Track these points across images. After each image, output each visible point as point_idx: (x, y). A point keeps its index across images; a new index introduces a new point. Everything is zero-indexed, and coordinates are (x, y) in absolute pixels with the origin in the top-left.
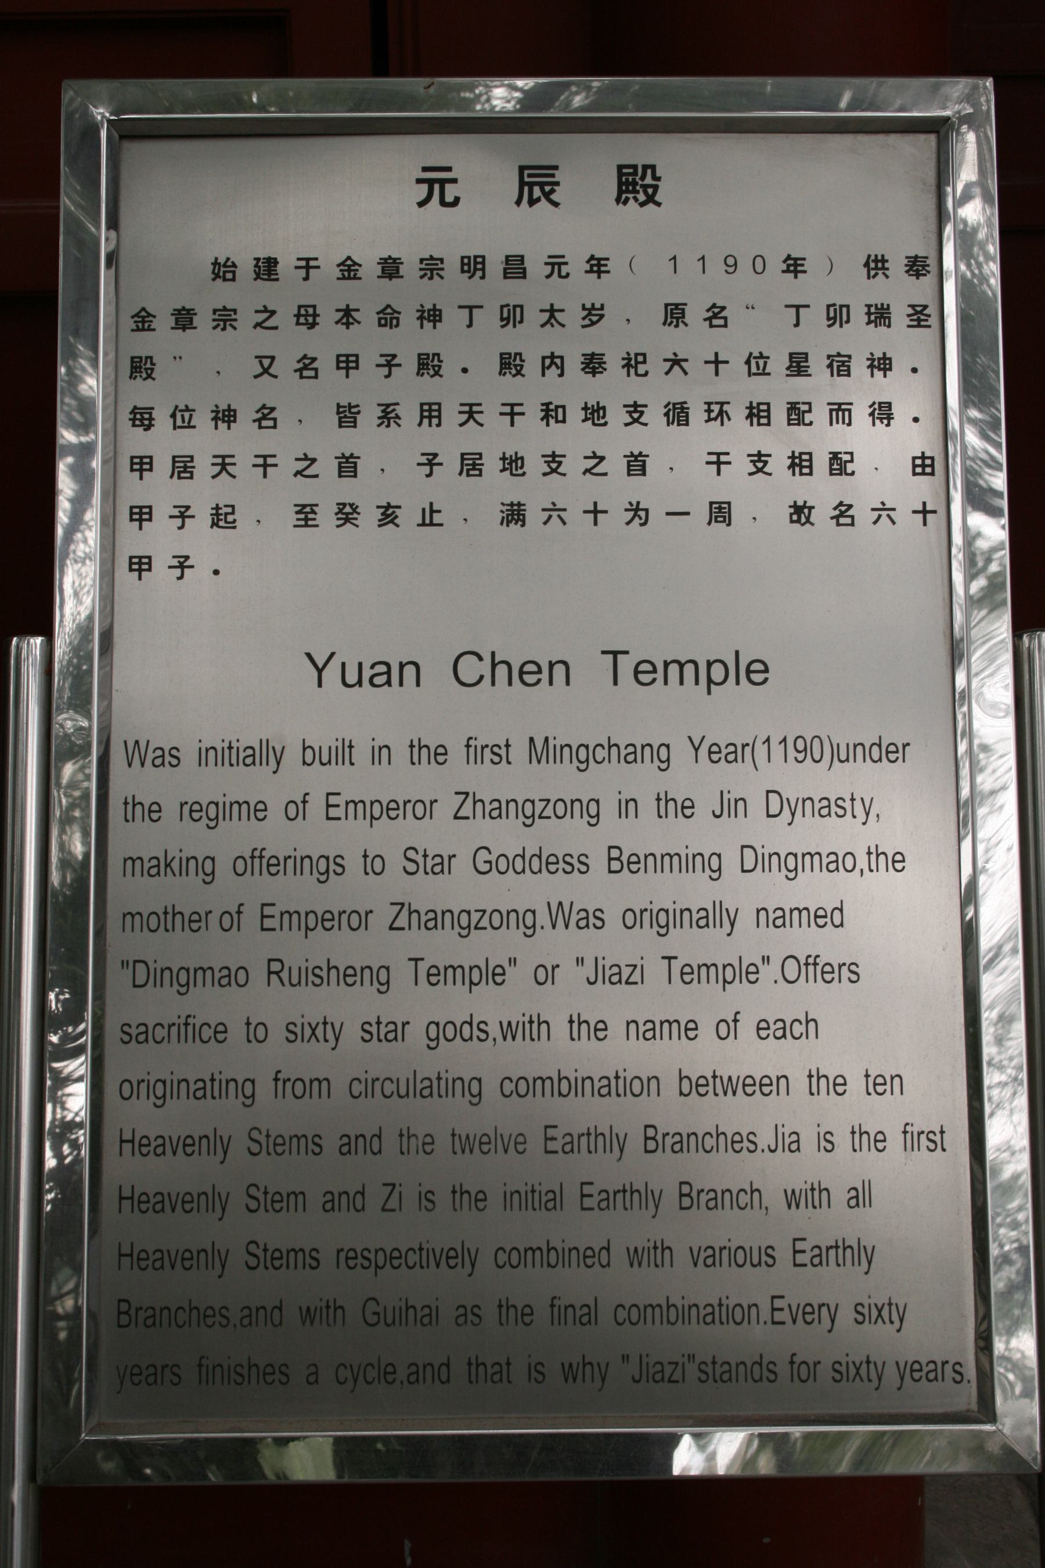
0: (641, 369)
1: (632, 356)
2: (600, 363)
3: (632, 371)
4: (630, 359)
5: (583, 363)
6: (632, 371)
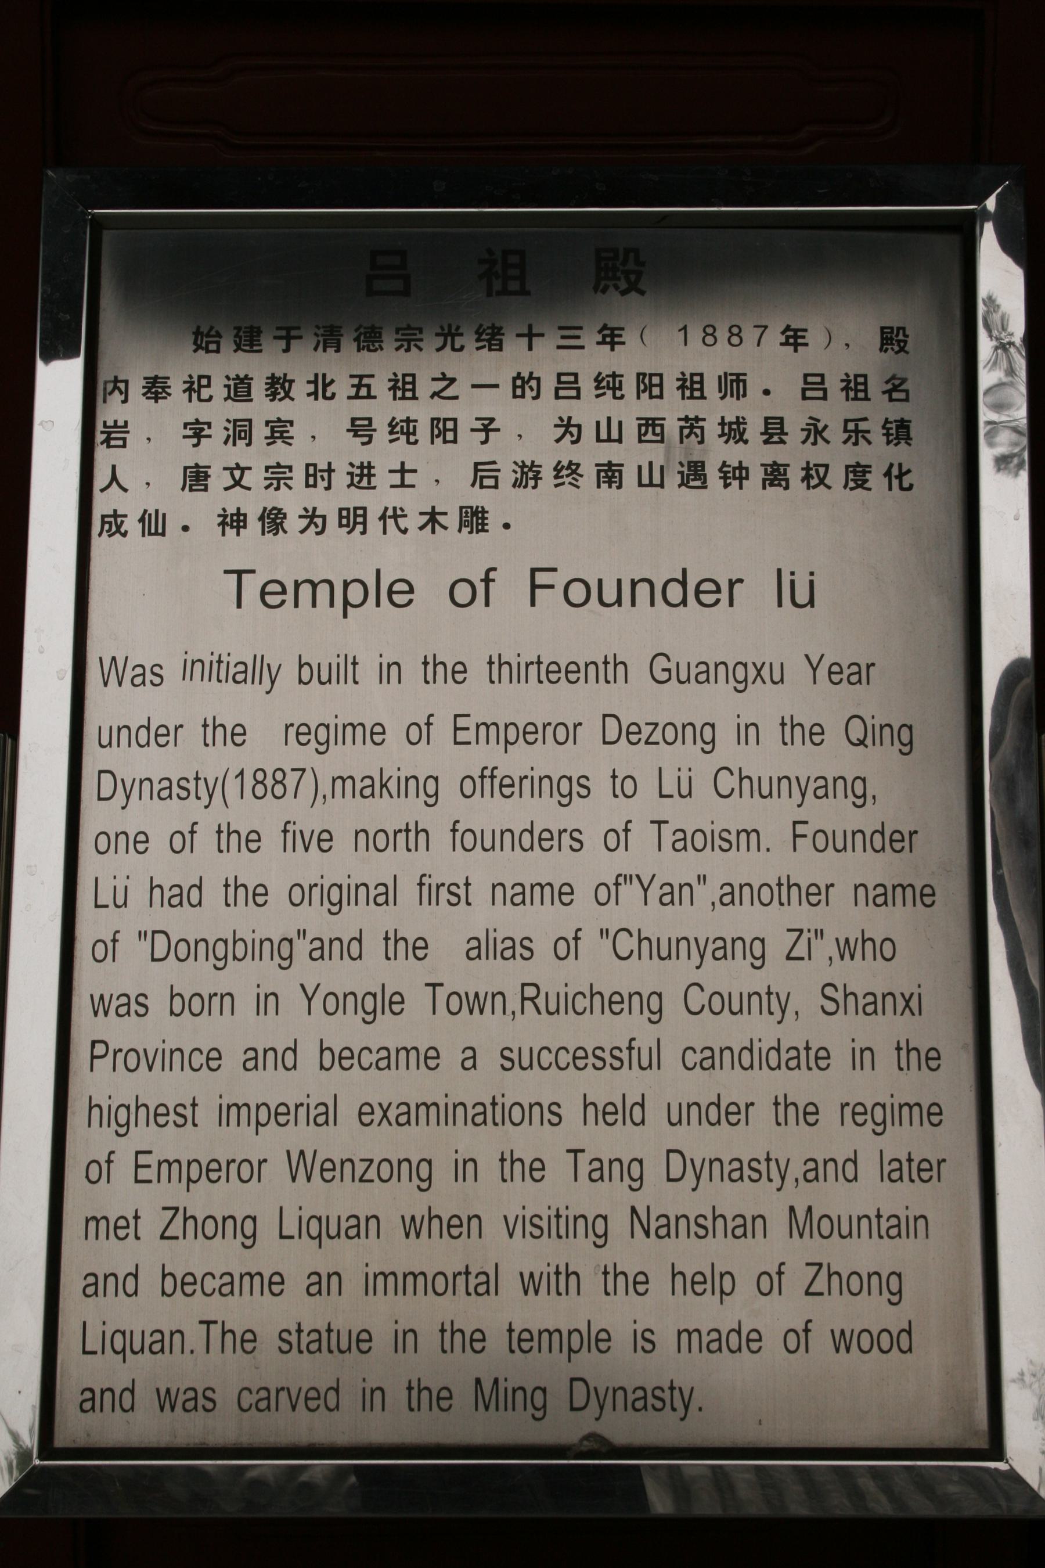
0: (205, 393)
2: (163, 388)
3: (194, 396)
5: (144, 387)
6: (194, 396)
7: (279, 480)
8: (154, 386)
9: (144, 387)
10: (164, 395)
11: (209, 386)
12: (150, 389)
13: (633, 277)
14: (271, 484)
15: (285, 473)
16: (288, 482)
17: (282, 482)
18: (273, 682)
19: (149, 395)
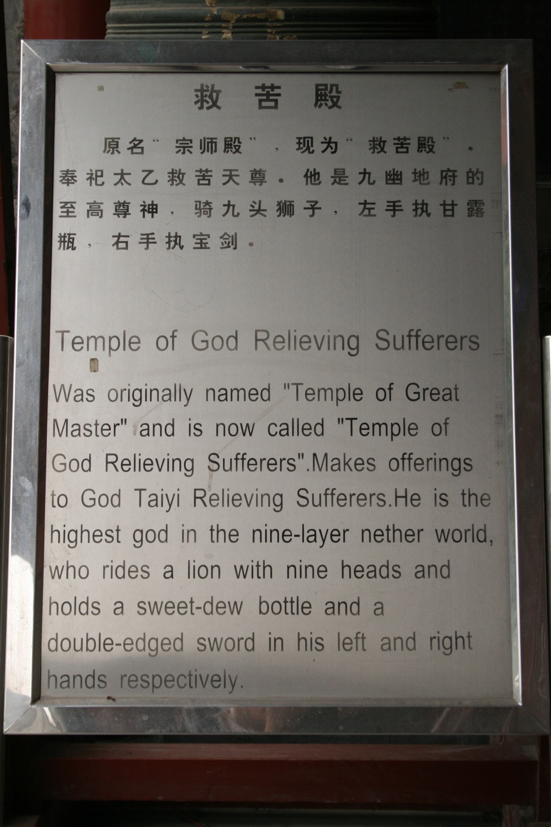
1: (94, 172)
2: (72, 177)
3: (93, 182)
4: (92, 174)
5: (60, 177)
6: (93, 182)
7: (184, 148)
8: (66, 176)
9: (60, 177)
10: (72, 181)
11: (102, 176)
12: (64, 177)
13: (335, 100)
14: (180, 150)
15: (188, 144)
16: (190, 149)
17: (186, 149)
18: (188, 400)
19: (64, 181)
